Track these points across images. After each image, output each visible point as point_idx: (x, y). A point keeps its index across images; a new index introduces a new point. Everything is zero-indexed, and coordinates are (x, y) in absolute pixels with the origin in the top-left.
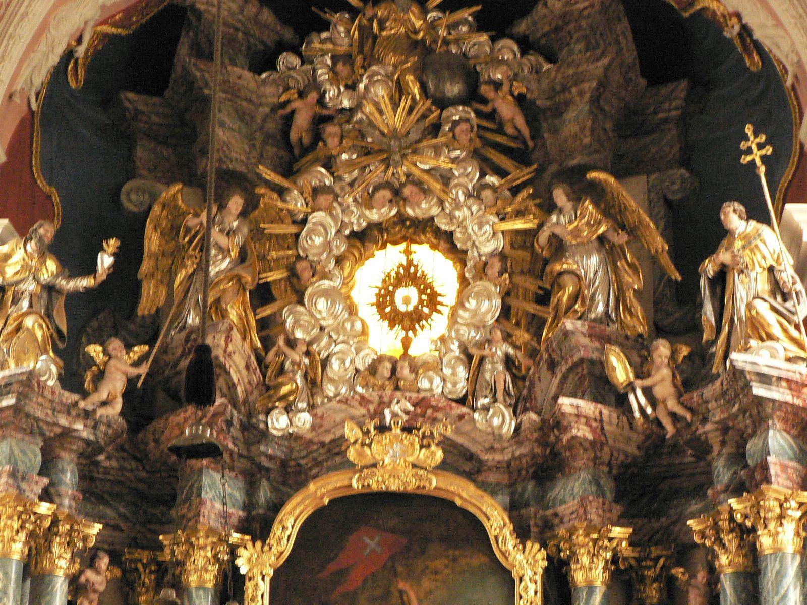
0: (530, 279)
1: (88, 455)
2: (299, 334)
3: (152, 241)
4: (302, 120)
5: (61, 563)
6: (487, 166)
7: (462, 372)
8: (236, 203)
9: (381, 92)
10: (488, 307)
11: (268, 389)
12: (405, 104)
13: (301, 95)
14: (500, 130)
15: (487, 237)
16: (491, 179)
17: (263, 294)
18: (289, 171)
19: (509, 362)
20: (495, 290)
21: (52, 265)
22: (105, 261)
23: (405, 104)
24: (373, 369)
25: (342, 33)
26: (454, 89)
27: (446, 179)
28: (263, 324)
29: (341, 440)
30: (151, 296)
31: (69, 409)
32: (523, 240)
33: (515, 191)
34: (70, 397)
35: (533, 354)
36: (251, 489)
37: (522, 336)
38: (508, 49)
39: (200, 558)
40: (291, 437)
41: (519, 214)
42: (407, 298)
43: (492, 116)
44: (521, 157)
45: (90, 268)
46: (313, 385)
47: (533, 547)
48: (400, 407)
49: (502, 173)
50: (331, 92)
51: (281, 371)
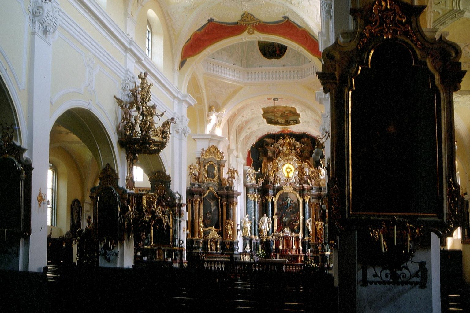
0: (301, 170)
1: (258, 189)
2: (278, 176)
3: (263, 166)
4: (277, 151)
5: (256, 200)
6: (297, 157)
7: (294, 180)
8: (271, 163)
9: (285, 149)
10: (297, 173)
11: (275, 182)
12: (288, 151)
13: (277, 149)
14: (298, 153)
15: (297, 165)
16: (297, 159)
17: (274, 171)
18: (276, 158)
19: (299, 179)
20: (297, 171)
21: (254, 171)
22: (259, 170)
23: (288, 151)
24: (285, 179)
25: (281, 141)
26: (293, 148)
27: (292, 159)
28: (274, 174)
29: (282, 187)
30: (263, 171)
31: (257, 186)
32: (300, 166)
33: (299, 161)
34: (257, 184)
35: (301, 179)
36: (274, 191)
37: (300, 177)
38: (298, 143)
39: (270, 198)
40: (278, 187)
41: (300, 163)
42: (289, 170)
43: (297, 151)
44: (300, 156)
45: (258, 171)
46: (279, 181)
47: (301, 198)
48: (288, 184)
49: (298, 158)
50: (280, 148)
51: (276, 180)
